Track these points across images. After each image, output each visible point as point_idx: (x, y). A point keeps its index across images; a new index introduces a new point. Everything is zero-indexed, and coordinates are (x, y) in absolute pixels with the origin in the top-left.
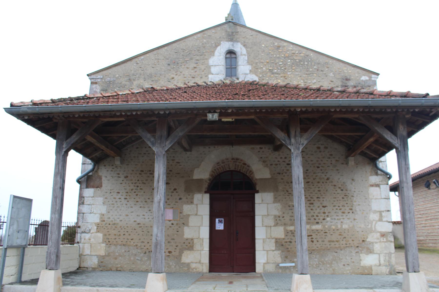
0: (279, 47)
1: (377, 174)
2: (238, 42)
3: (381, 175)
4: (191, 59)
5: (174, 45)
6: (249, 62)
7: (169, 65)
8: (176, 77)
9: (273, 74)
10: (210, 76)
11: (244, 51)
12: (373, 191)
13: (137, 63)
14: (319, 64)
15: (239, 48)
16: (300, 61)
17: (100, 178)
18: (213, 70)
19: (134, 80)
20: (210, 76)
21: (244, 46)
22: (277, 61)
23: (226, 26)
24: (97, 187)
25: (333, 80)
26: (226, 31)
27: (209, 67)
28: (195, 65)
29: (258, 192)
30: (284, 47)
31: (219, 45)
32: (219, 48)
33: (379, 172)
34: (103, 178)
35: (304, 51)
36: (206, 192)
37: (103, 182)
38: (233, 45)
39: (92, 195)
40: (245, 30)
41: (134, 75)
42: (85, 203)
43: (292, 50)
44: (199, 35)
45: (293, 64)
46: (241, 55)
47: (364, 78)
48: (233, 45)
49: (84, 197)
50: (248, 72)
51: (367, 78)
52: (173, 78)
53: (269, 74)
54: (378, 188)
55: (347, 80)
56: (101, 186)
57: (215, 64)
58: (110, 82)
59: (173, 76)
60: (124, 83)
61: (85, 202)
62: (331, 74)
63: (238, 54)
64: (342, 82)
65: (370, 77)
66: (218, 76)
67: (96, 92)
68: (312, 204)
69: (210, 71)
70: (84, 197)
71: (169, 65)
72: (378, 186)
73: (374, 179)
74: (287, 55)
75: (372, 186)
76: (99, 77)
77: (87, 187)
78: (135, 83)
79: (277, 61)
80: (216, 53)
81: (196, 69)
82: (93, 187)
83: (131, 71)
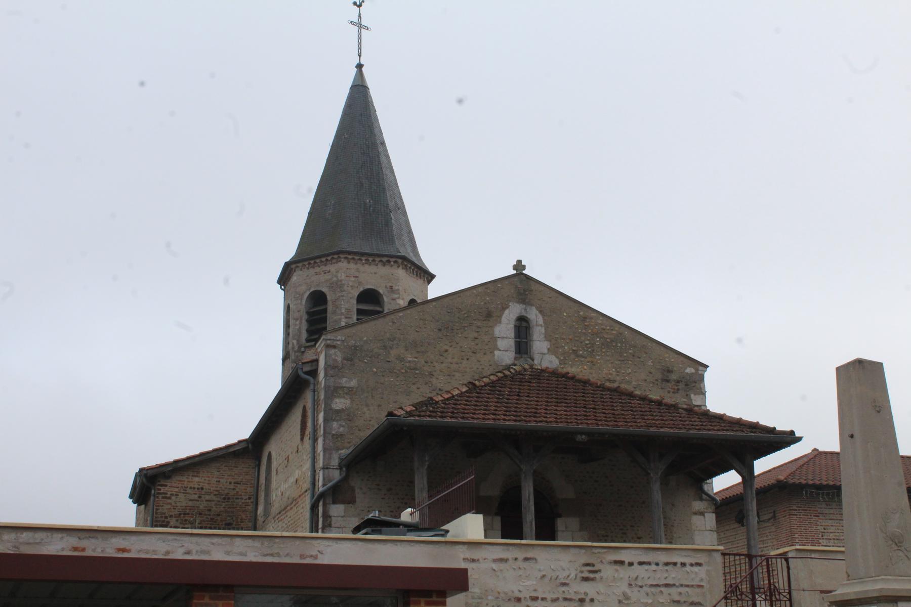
0: (585, 318)
1: (701, 499)
2: (532, 305)
3: (706, 500)
4: (471, 324)
5: (445, 300)
6: (547, 337)
7: (440, 330)
8: (450, 349)
9: (578, 356)
10: (496, 353)
11: (541, 321)
12: (697, 520)
13: (394, 323)
14: (635, 347)
15: (533, 315)
16: (612, 341)
17: (353, 490)
18: (501, 344)
19: (391, 348)
20: (496, 353)
21: (541, 312)
22: (583, 338)
23: (516, 279)
24: (349, 503)
25: (652, 371)
26: (516, 287)
27: (494, 339)
28: (476, 335)
29: (560, 516)
30: (591, 318)
31: (507, 307)
32: (507, 311)
33: (704, 496)
34: (357, 490)
35: (617, 327)
36: (497, 514)
37: (357, 495)
38: (525, 309)
39: (343, 514)
40: (542, 288)
41: (389, 339)
42: (333, 525)
43: (602, 324)
44: (480, 290)
45: (603, 344)
46: (537, 325)
47: (689, 370)
48: (525, 309)
49: (330, 517)
50: (546, 351)
51: (693, 371)
52: (446, 351)
53: (573, 356)
54: (702, 517)
55: (669, 371)
56: (355, 501)
57: (502, 335)
58: (356, 347)
59: (446, 347)
60: (376, 350)
61: (333, 523)
62: (650, 363)
63: (533, 323)
64: (663, 374)
65: (697, 370)
66: (507, 353)
67: (335, 360)
68: (625, 534)
69: (496, 345)
70: (330, 517)
71: (440, 330)
72: (702, 514)
73: (698, 505)
74: (595, 331)
75: (695, 514)
76: (339, 338)
77: (334, 502)
78: (393, 352)
79: (583, 338)
80: (504, 319)
81: (477, 341)
82: (343, 502)
83: (385, 333)
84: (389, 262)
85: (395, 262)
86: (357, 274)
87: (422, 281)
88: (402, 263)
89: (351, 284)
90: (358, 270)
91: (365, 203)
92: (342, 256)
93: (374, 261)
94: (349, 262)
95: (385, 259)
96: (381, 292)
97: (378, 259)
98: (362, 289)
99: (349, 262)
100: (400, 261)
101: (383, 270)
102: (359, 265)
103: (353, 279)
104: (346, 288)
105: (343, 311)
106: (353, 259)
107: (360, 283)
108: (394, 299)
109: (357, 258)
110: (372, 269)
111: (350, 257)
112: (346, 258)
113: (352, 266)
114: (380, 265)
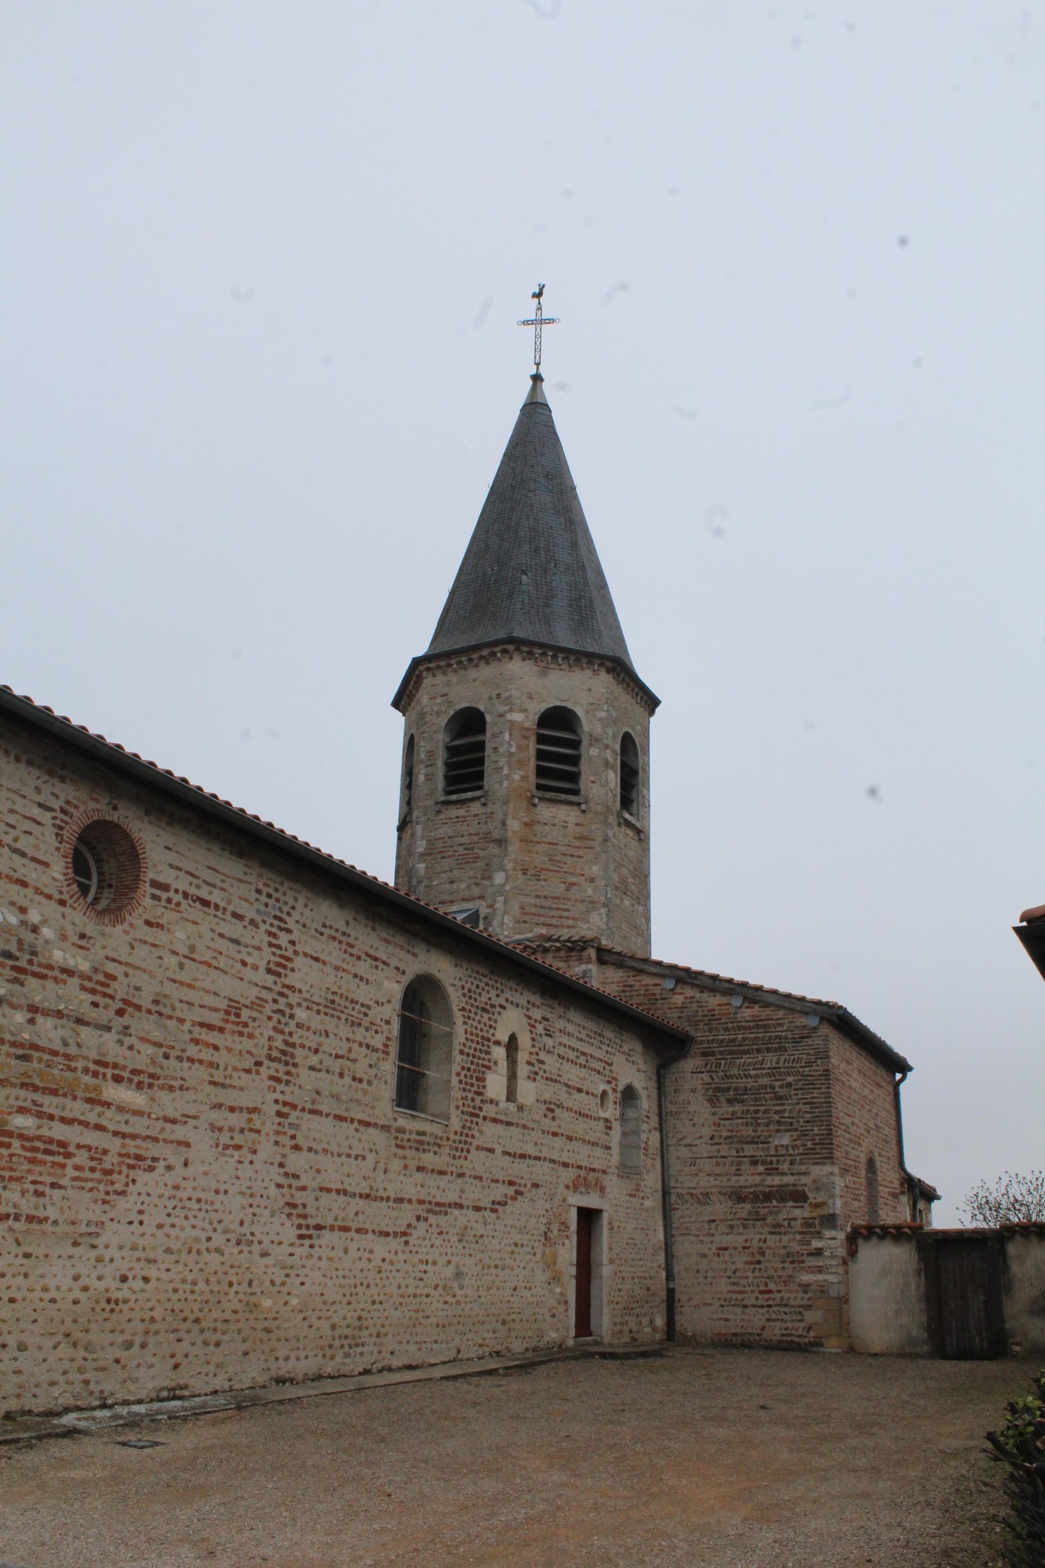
84: (494, 654)
85: (505, 652)
86: (446, 690)
87: (588, 673)
88: (517, 649)
89: (436, 709)
90: (448, 684)
91: (485, 574)
92: (422, 668)
93: (470, 660)
94: (434, 675)
95: (485, 652)
96: (482, 708)
97: (475, 656)
98: (452, 713)
99: (434, 675)
100: (511, 648)
101: (486, 672)
102: (453, 678)
103: (439, 700)
104: (428, 718)
105: (423, 756)
106: (439, 667)
107: (450, 703)
108: (501, 716)
109: (443, 663)
110: (472, 673)
111: (432, 665)
112: (428, 669)
113: (440, 679)
114: (482, 664)
